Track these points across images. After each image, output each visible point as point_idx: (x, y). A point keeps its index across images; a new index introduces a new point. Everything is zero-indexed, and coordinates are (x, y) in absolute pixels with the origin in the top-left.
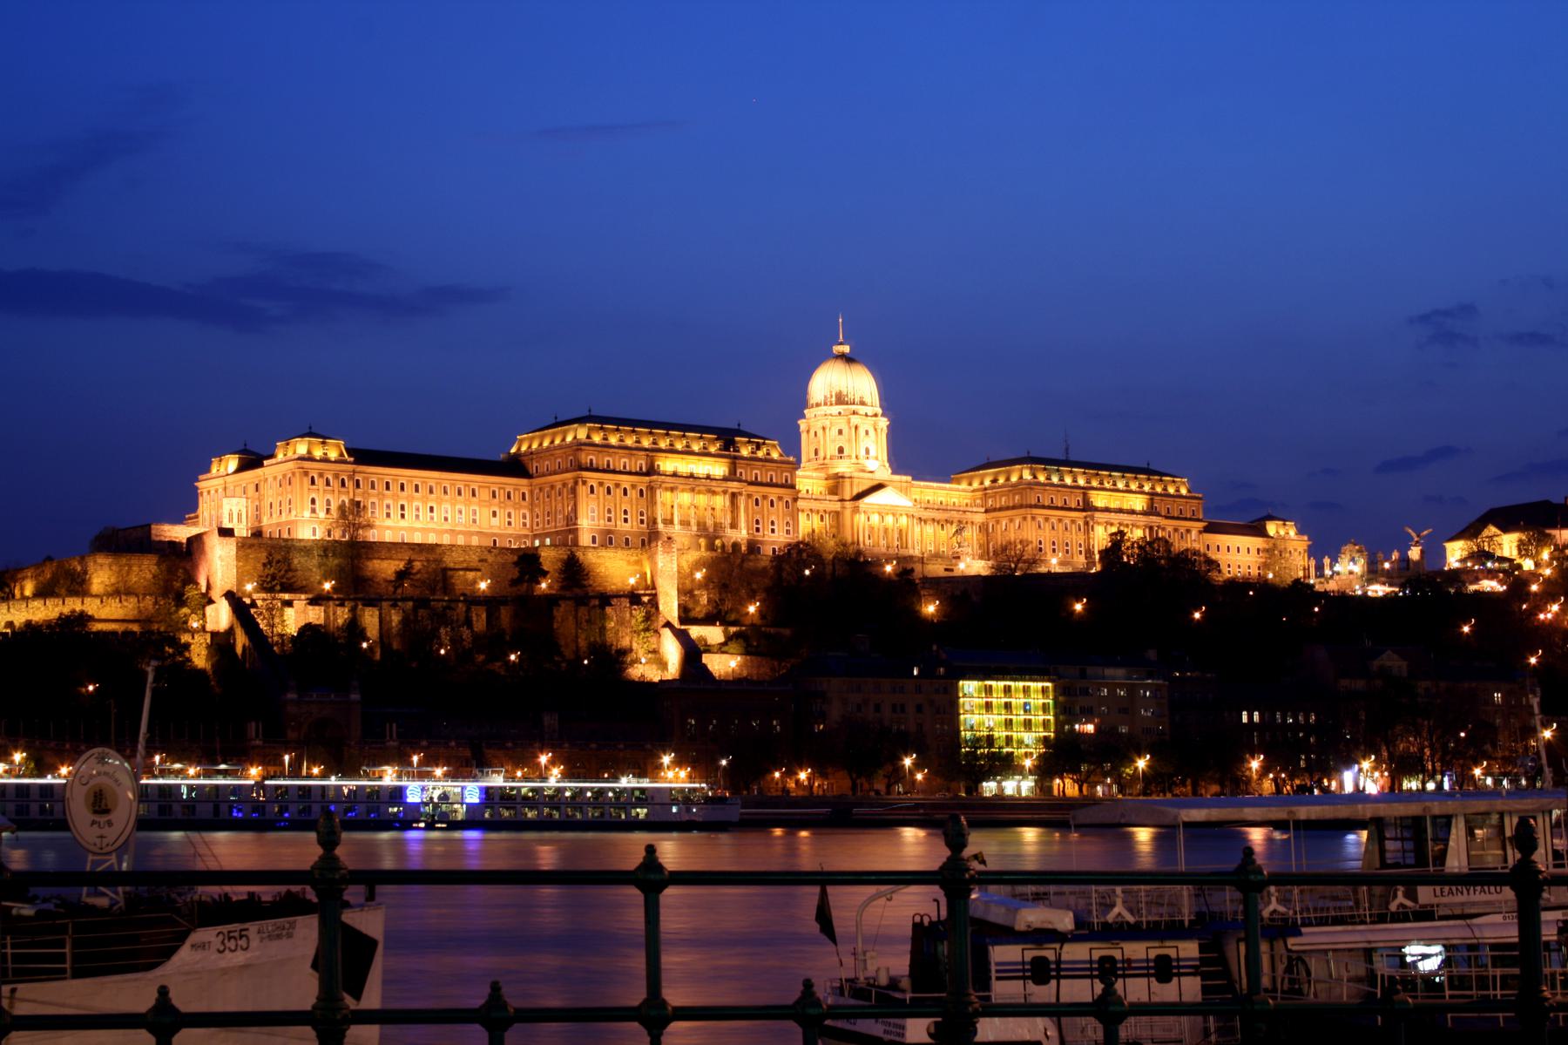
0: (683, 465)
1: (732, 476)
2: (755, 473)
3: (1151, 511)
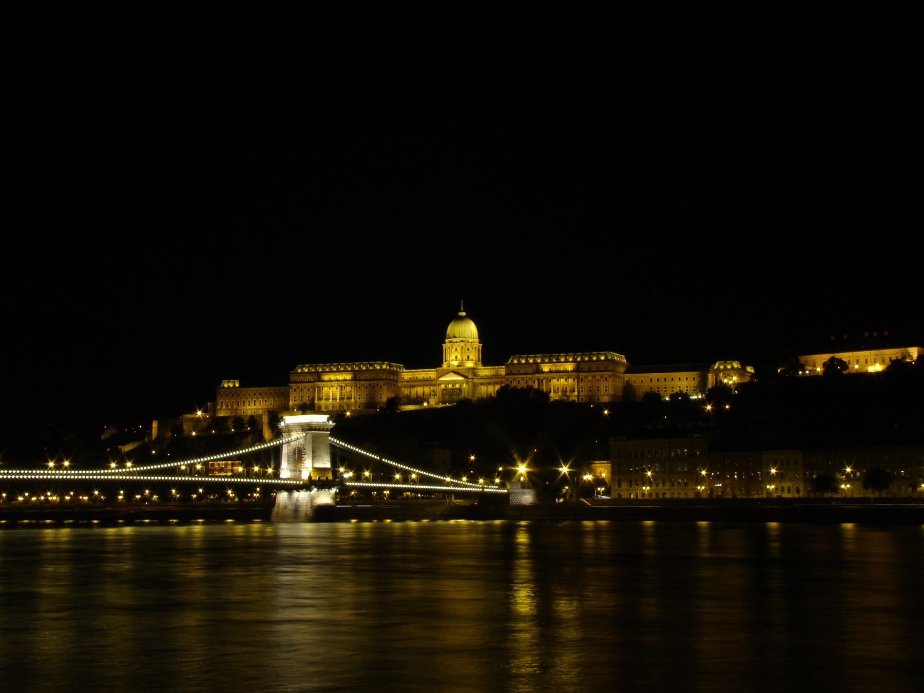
0: (332, 377)
1: (355, 379)
2: (363, 377)
3: (577, 370)
